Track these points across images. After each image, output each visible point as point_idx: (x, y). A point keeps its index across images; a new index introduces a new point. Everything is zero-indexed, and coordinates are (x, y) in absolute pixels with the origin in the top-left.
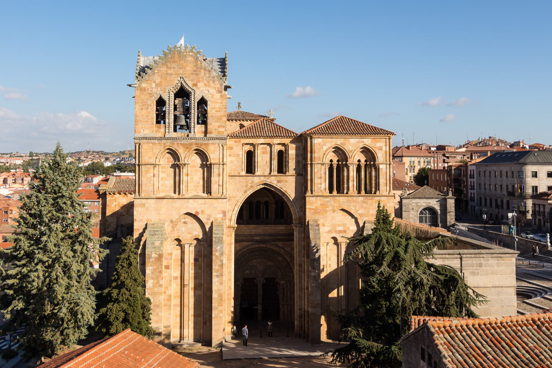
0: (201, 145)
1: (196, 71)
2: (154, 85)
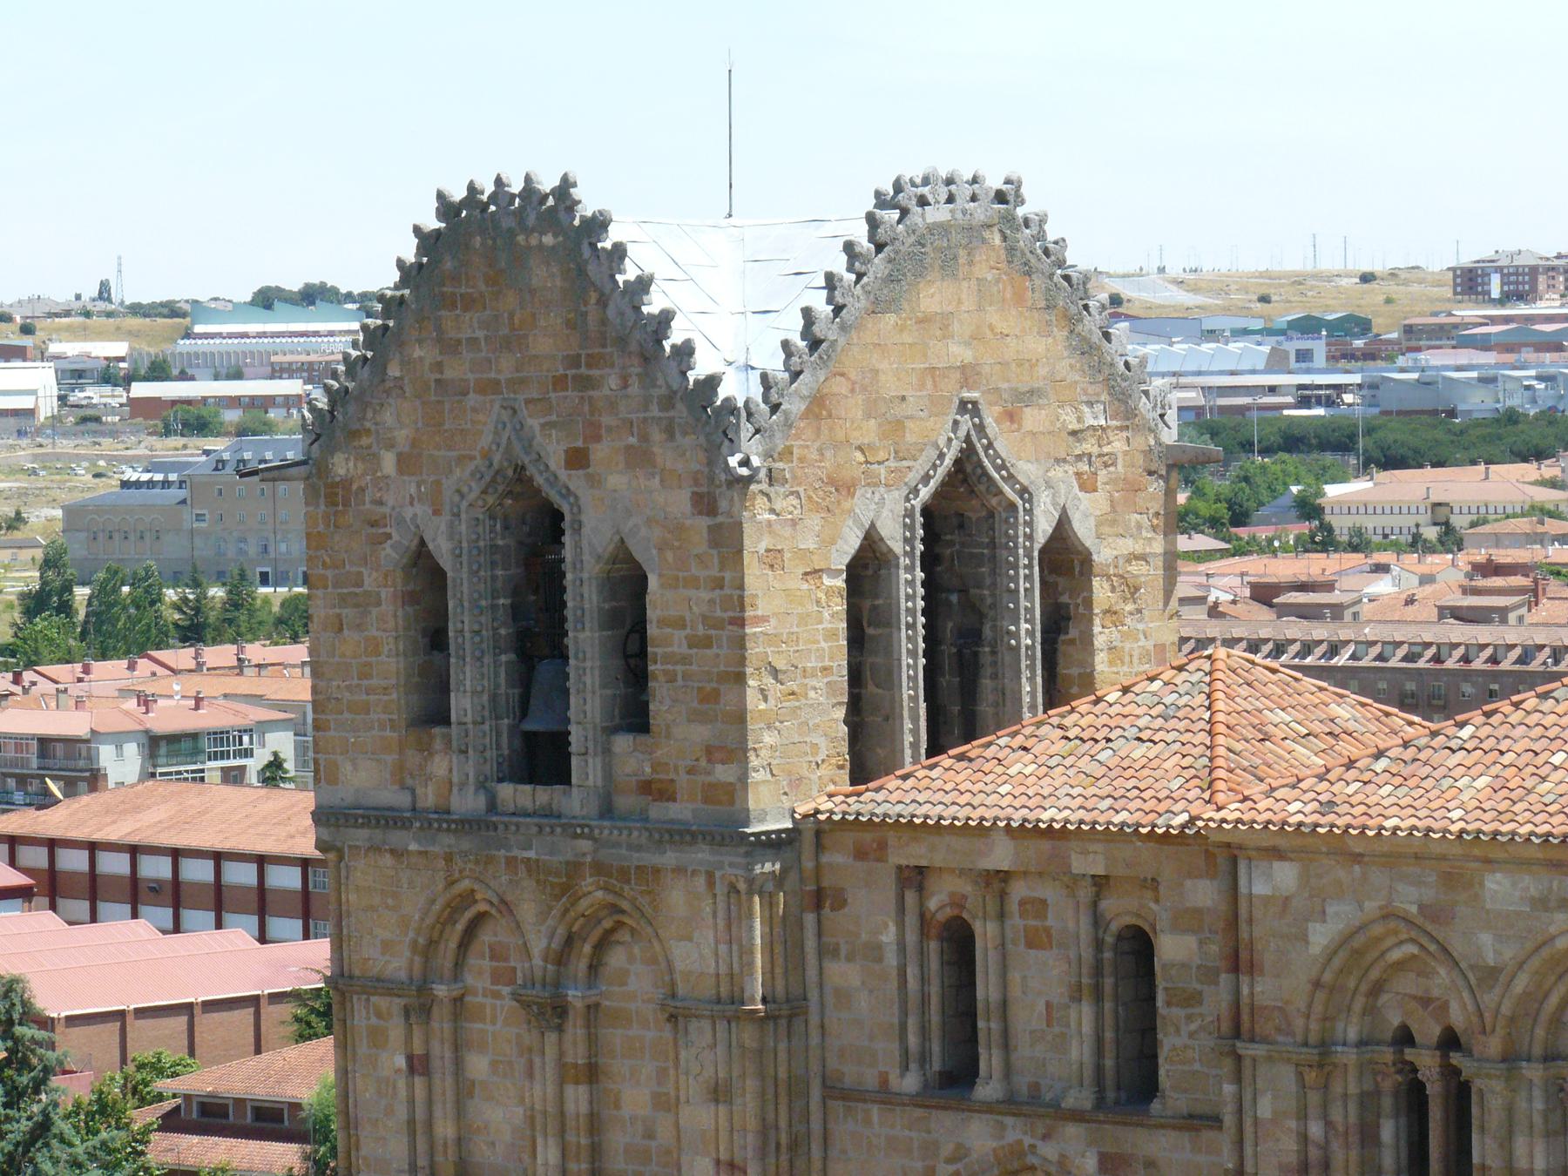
0: (624, 875)
1: (574, 362)
2: (389, 462)
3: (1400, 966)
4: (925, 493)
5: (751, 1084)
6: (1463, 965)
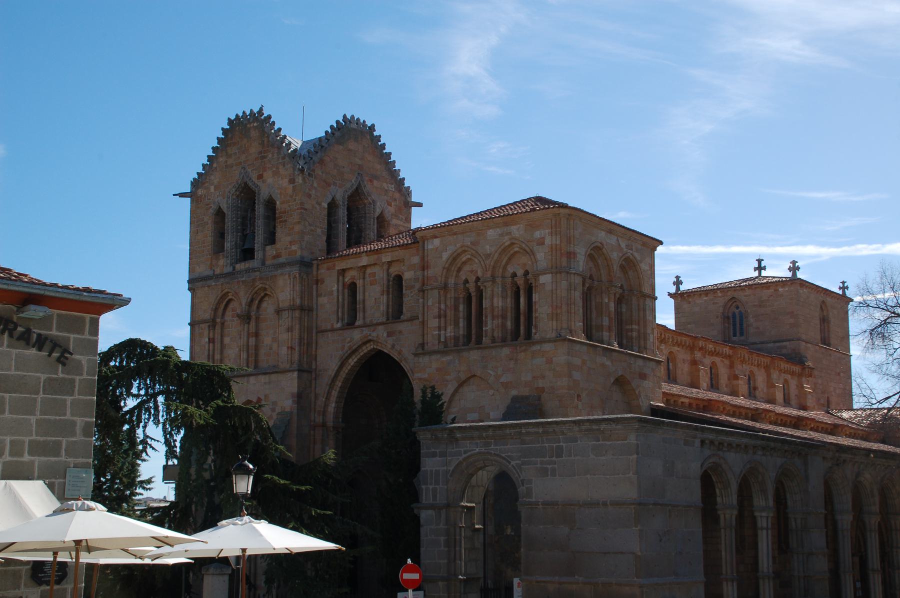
1: (260, 153)
3: (464, 263)
4: (349, 193)
5: (297, 326)
6: (481, 255)
